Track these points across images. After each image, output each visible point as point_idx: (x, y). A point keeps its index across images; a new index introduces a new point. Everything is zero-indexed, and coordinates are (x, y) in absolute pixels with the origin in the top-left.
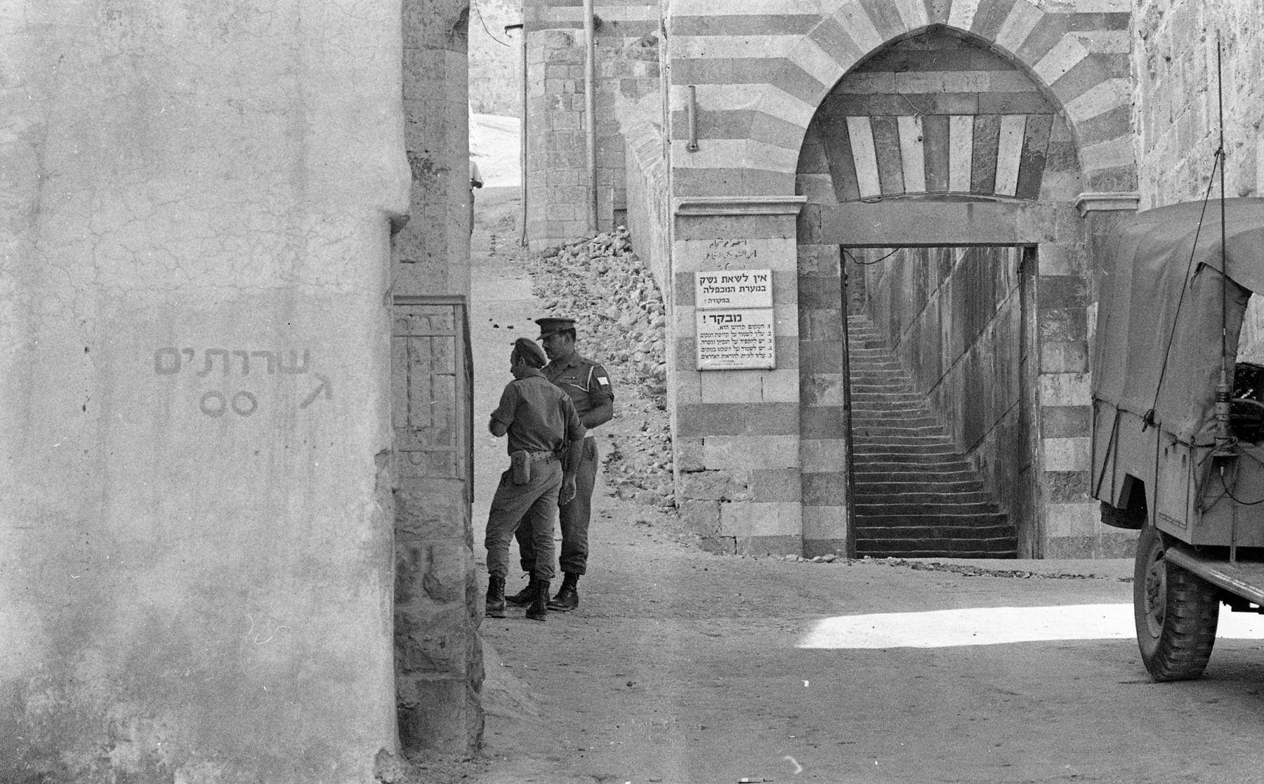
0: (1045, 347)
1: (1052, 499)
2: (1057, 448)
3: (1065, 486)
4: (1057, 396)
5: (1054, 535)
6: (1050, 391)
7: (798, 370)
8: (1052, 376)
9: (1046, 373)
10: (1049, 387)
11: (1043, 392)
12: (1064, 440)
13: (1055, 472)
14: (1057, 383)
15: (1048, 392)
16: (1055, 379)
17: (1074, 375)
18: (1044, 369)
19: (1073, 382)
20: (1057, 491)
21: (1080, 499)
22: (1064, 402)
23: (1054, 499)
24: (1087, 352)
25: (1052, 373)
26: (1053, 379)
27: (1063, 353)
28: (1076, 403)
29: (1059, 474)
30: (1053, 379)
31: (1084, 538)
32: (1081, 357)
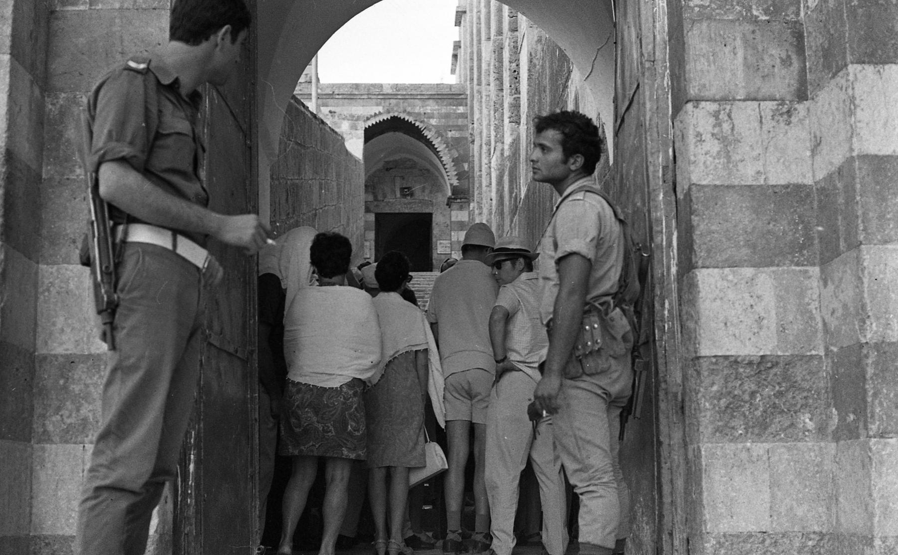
0: (696, 31)
1: (717, 430)
2: (731, 295)
3: (753, 394)
4: (728, 157)
5: (724, 527)
6: (713, 146)
7: (7, 57)
8: (712, 107)
9: (697, 101)
10: (707, 137)
11: (692, 147)
12: (748, 272)
13: (726, 357)
14: (726, 126)
15: (707, 146)
16: (723, 116)
17: (770, 105)
18: (693, 91)
19: (768, 124)
20: (731, 410)
21: (791, 432)
22: (747, 174)
23: (723, 431)
24: (800, 49)
25: (714, 100)
26: (716, 115)
27: (740, 53)
28: (778, 177)
29: (734, 362)
30: (716, 115)
31: (806, 536)
32: (786, 62)
